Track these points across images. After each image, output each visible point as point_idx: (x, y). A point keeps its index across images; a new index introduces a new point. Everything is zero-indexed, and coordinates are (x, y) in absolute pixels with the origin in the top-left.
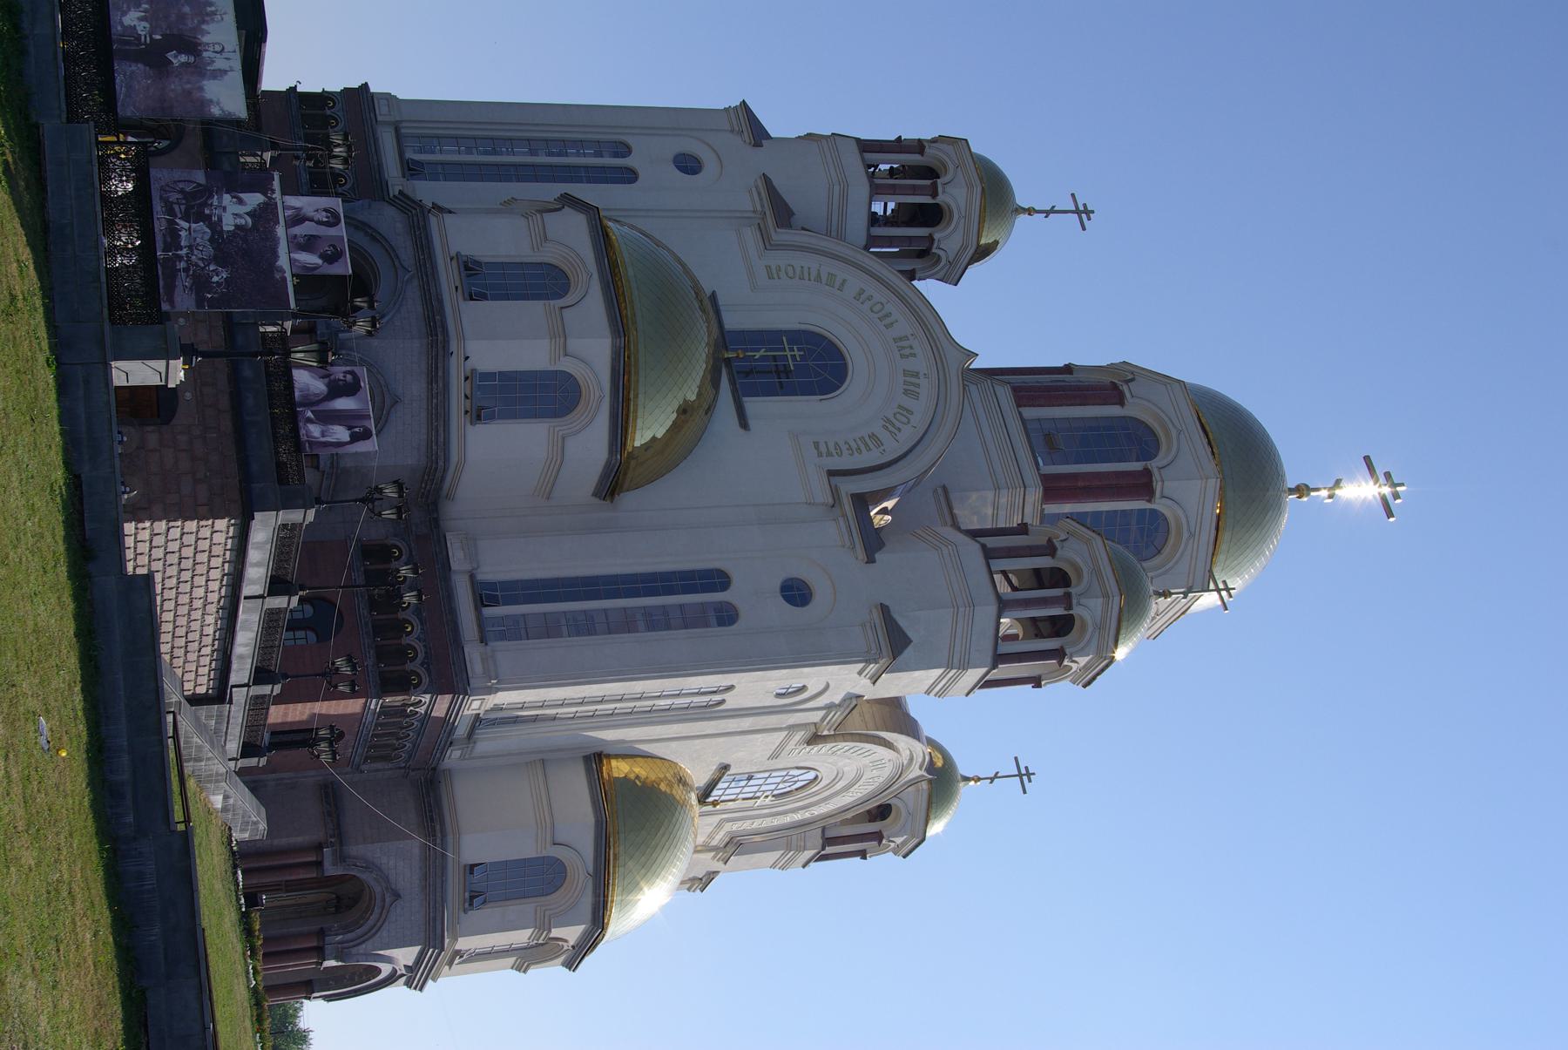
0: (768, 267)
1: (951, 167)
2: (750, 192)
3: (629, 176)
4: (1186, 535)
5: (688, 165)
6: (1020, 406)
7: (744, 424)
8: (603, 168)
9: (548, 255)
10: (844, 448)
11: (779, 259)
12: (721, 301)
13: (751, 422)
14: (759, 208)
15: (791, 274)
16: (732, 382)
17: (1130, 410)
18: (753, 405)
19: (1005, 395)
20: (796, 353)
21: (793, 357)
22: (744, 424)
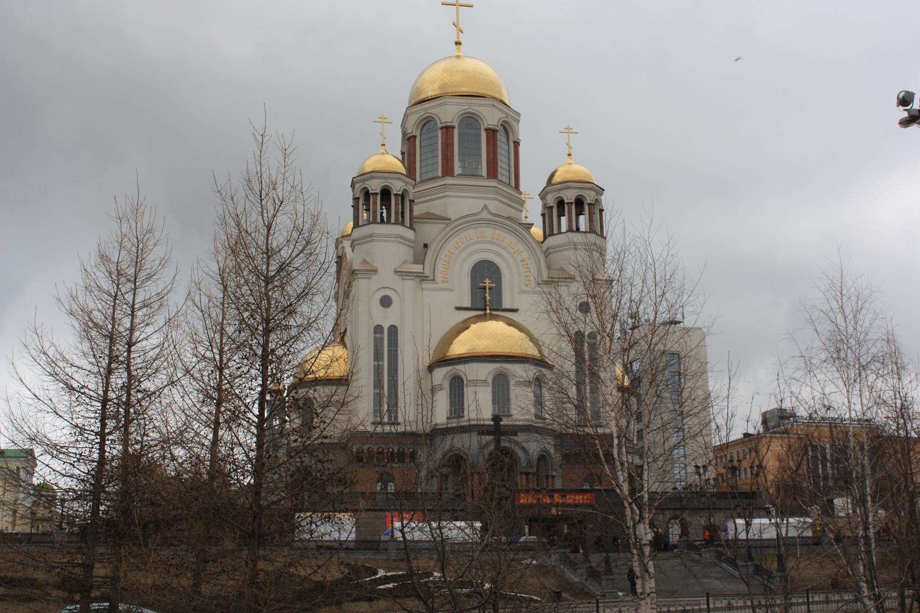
0: (443, 282)
1: (386, 184)
2: (403, 279)
3: (393, 330)
4: (507, 119)
5: (386, 302)
6: (453, 173)
7: (515, 310)
8: (389, 340)
9: (490, 381)
10: (527, 274)
11: (439, 276)
12: (459, 305)
13: (515, 307)
14: (413, 278)
15: (445, 273)
16: (497, 310)
17: (455, 124)
18: (506, 304)
19: (449, 181)
20: (487, 281)
21: (489, 283)
22: (515, 310)
